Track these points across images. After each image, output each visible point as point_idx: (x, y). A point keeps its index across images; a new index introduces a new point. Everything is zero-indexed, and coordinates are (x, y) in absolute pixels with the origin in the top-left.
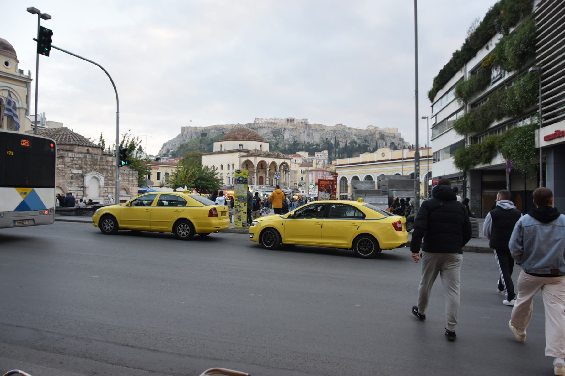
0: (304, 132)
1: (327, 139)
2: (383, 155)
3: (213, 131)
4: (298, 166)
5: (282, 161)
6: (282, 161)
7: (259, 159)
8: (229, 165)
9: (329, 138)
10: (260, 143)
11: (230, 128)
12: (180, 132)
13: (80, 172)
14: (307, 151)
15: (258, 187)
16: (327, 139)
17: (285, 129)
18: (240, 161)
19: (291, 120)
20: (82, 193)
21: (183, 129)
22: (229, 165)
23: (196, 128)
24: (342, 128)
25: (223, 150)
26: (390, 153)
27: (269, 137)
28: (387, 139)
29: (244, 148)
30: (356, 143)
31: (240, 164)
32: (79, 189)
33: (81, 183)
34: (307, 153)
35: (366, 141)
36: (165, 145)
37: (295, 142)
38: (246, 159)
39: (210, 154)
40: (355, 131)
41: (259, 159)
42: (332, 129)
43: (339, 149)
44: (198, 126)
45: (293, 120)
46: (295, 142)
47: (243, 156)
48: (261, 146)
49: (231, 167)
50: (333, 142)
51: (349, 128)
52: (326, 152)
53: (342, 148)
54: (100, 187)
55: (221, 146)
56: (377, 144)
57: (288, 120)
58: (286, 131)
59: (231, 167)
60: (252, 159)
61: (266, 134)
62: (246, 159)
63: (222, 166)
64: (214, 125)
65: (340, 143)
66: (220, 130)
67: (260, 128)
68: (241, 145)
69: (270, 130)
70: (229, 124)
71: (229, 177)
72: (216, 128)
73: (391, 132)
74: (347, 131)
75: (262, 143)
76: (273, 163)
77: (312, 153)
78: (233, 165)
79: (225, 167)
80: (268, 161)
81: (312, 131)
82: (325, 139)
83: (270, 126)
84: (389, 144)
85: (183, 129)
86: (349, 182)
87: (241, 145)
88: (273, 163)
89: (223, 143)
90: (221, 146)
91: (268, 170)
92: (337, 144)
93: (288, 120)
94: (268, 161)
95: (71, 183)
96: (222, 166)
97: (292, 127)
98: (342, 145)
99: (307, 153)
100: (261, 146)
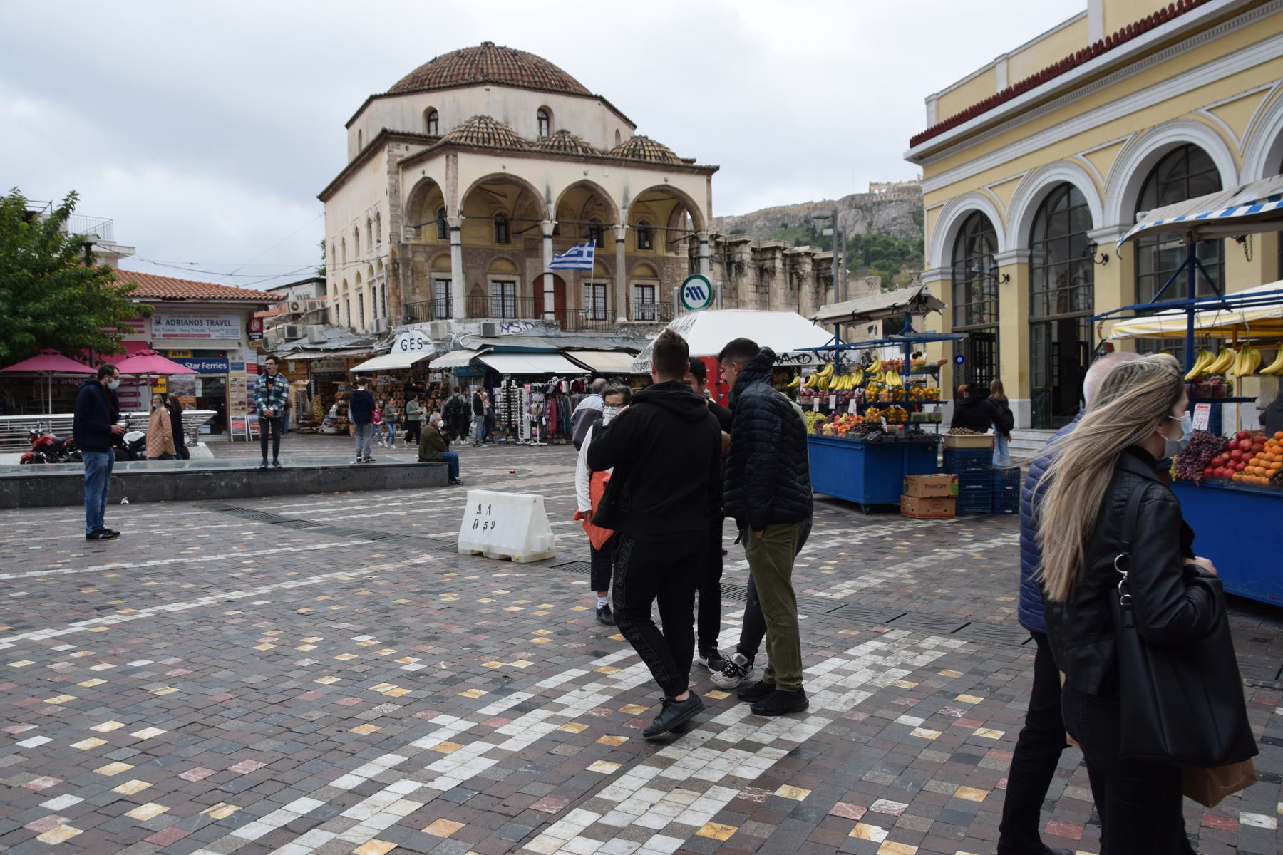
3: (759, 223)
7: (474, 168)
10: (537, 99)
15: (474, 327)
18: (394, 192)
27: (903, 228)
31: (394, 206)
41: (474, 168)
44: (724, 215)
48: (545, 114)
61: (895, 219)
64: (763, 208)
66: (778, 220)
67: (879, 204)
68: (431, 115)
69: (906, 207)
70: (800, 202)
72: (766, 214)
76: (586, 190)
83: (905, 196)
87: (431, 115)
88: (586, 190)
91: (548, 228)
100: (545, 114)
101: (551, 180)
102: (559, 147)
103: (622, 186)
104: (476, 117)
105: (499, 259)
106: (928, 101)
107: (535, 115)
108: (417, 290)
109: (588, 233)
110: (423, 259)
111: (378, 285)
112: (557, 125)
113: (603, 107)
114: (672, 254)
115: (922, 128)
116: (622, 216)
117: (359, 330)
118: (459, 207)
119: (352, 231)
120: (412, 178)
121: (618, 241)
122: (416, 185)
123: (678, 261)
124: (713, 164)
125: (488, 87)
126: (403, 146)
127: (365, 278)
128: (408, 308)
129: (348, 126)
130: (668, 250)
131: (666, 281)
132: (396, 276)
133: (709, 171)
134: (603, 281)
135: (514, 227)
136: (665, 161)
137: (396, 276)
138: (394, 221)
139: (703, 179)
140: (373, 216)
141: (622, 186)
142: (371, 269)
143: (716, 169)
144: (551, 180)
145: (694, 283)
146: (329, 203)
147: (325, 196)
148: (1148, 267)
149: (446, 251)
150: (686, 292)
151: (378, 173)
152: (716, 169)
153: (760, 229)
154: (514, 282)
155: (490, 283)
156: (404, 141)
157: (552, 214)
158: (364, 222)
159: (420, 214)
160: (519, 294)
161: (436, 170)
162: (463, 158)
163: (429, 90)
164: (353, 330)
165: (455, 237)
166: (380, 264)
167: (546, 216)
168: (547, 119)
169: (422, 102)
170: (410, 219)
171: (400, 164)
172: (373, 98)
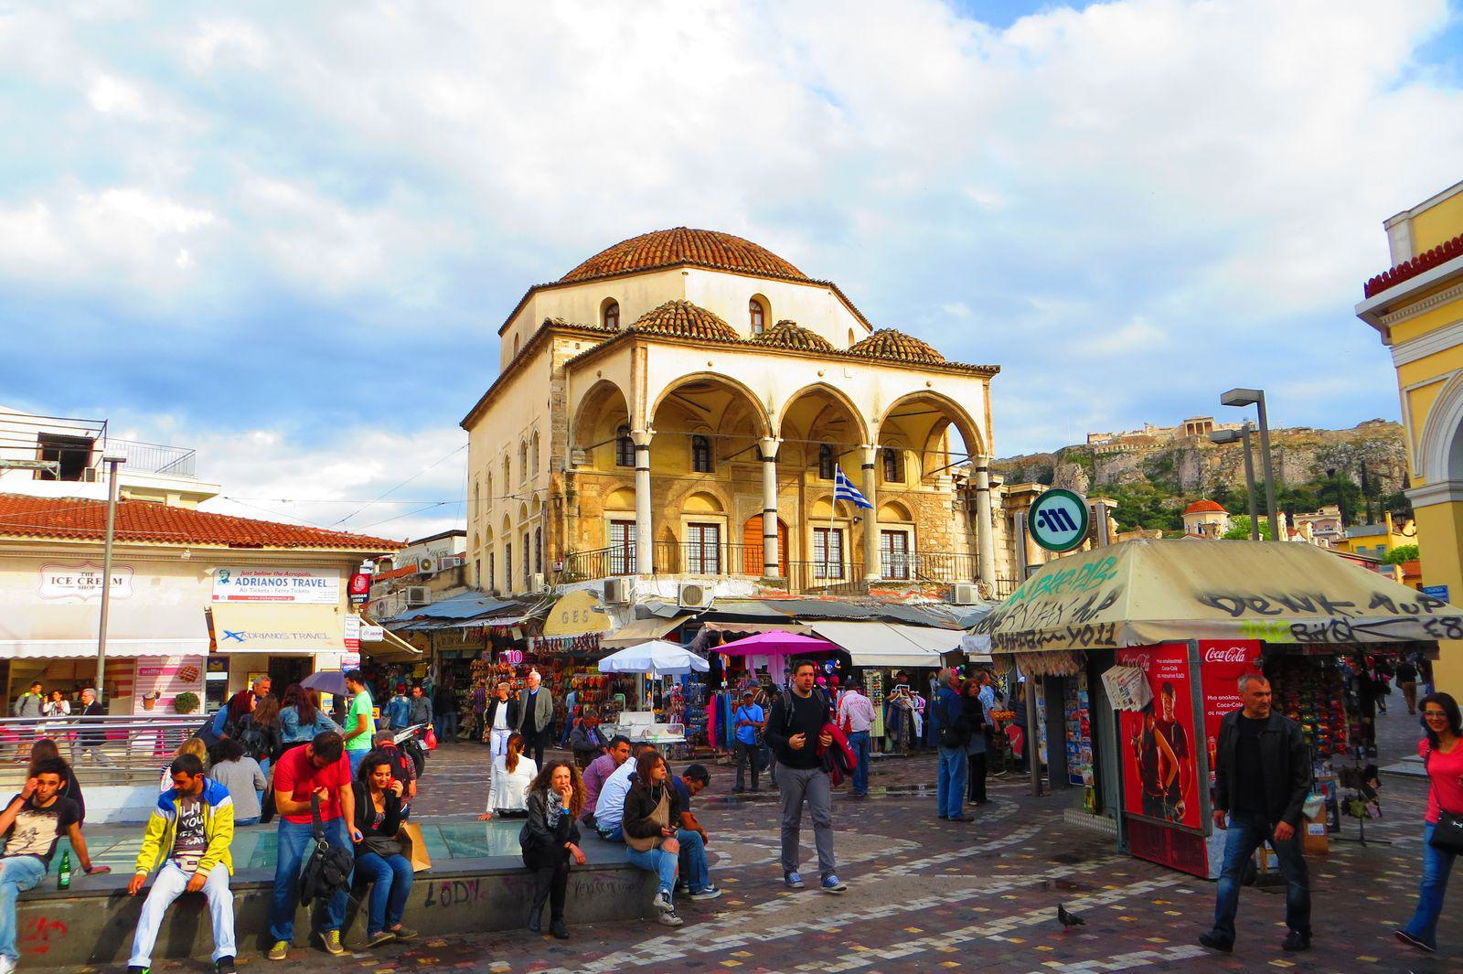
1: (1331, 472)
9: (1338, 470)
10: (752, 286)
17: (1182, 453)
18: (558, 403)
19: (1199, 426)
24: (1386, 430)
45: (1208, 425)
48: (759, 305)
57: (1190, 427)
65: (1385, 481)
68: (610, 308)
69: (1134, 460)
75: (772, 289)
87: (610, 308)
91: (771, 447)
93: (1190, 427)
100: (759, 305)
101: (774, 383)
102: (784, 340)
103: (873, 392)
104: (671, 303)
105: (697, 494)
106: (1389, 225)
107: (746, 306)
108: (585, 536)
109: (817, 460)
110: (594, 494)
111: (532, 532)
112: (777, 315)
113: (834, 299)
114: (930, 489)
115: (1384, 265)
116: (873, 431)
117: (505, 594)
118: (650, 418)
119: (501, 460)
121: (865, 467)
122: (589, 392)
123: (938, 498)
124: (990, 363)
125: (685, 270)
126: (572, 343)
127: (515, 522)
129: (501, 332)
130: (925, 484)
131: (922, 524)
133: (987, 372)
134: (839, 525)
135: (716, 451)
136: (923, 359)
139: (978, 383)
140: (528, 437)
141: (873, 392)
142: (524, 508)
143: (994, 371)
144: (774, 383)
145: (1046, 505)
146: (475, 430)
147: (468, 423)
149: (630, 484)
150: (1038, 518)
151: (538, 381)
152: (994, 371)
154: (717, 526)
155: (685, 526)
156: (574, 336)
157: (776, 427)
158: (516, 447)
159: (592, 432)
160: (724, 539)
161: (614, 370)
162: (651, 347)
163: (608, 277)
164: (496, 594)
165: (643, 459)
166: (536, 500)
168: (761, 312)
169: (597, 293)
170: (579, 439)
171: (567, 365)
172: (534, 290)
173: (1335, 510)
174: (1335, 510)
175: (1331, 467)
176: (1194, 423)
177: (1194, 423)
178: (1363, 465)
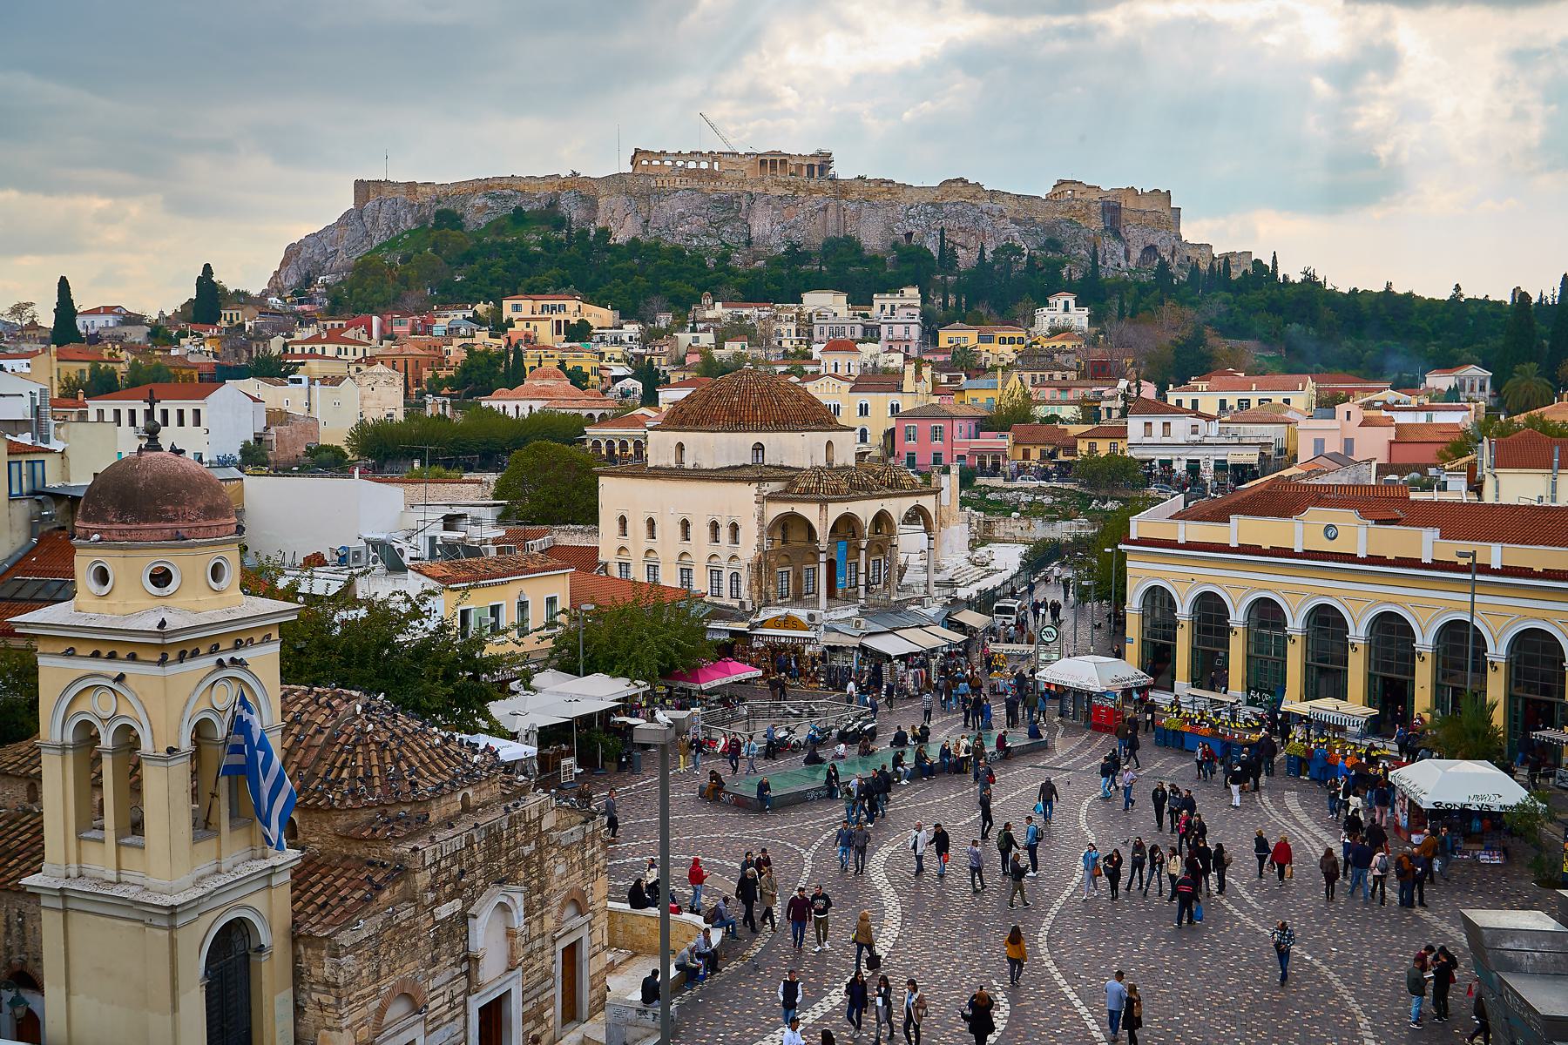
0: (825, 209)
1: (909, 235)
2: (1330, 532)
4: (847, 386)
5: (909, 503)
6: (909, 503)
7: (836, 510)
8: (715, 527)
10: (825, 436)
11: (543, 191)
12: (349, 203)
13: (457, 904)
14: (838, 287)
16: (909, 235)
18: (761, 518)
20: (463, 982)
21: (362, 188)
22: (715, 527)
23: (411, 186)
24: (967, 192)
25: (688, 464)
26: (1362, 531)
28: (1132, 233)
29: (771, 458)
30: (1018, 251)
32: (457, 971)
33: (459, 948)
34: (843, 298)
35: (1053, 244)
36: (292, 252)
37: (793, 247)
38: (785, 508)
39: (633, 476)
40: (1013, 205)
41: (836, 510)
42: (930, 197)
43: (959, 274)
45: (784, 162)
46: (793, 247)
47: (772, 498)
49: (724, 533)
50: (932, 246)
51: (993, 194)
52: (912, 293)
53: (968, 273)
54: (510, 934)
55: (681, 447)
56: (1095, 256)
58: (759, 204)
59: (724, 533)
60: (810, 511)
61: (682, 216)
62: (785, 508)
63: (685, 525)
65: (960, 252)
68: (759, 448)
71: (715, 573)
73: (1144, 206)
74: (985, 204)
77: (860, 298)
78: (734, 528)
79: (700, 531)
80: (865, 510)
81: (853, 207)
82: (900, 234)
84: (1136, 254)
85: (363, 189)
86: (1184, 611)
87: (759, 448)
88: (881, 519)
89: (688, 438)
90: (681, 447)
92: (948, 257)
93: (763, 163)
94: (865, 510)
95: (435, 961)
96: (685, 525)
97: (780, 191)
98: (966, 258)
99: (843, 298)
120: (775, 510)
128: (767, 595)
132: (760, 573)
137: (760, 573)
138: (760, 536)
148: (1252, 639)
153: (479, 210)
167: (863, 537)
173: (915, 291)
174: (915, 291)
175: (909, 229)
176: (769, 158)
177: (769, 158)
178: (942, 234)
